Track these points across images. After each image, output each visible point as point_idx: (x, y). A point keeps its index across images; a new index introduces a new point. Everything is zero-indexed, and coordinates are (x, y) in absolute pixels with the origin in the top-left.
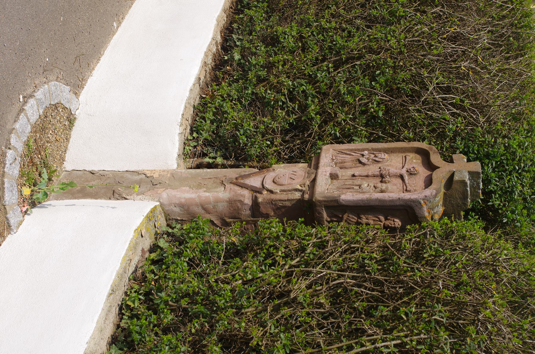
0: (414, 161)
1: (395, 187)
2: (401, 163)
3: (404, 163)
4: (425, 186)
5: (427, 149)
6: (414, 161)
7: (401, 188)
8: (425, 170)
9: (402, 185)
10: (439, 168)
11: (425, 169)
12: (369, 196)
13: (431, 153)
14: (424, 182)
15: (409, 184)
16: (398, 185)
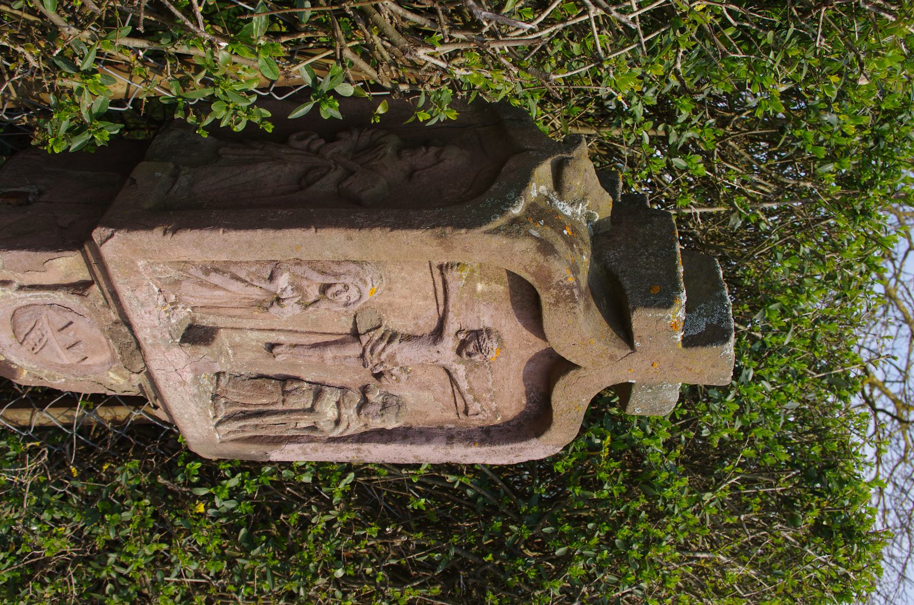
0: (480, 287)
1: (426, 395)
2: (431, 293)
3: (441, 301)
4: (527, 394)
5: (530, 279)
6: (480, 287)
7: (449, 399)
8: (525, 332)
9: (450, 390)
10: (575, 367)
11: (526, 326)
12: (354, 454)
13: (546, 298)
14: (524, 380)
15: (471, 390)
16: (439, 389)
